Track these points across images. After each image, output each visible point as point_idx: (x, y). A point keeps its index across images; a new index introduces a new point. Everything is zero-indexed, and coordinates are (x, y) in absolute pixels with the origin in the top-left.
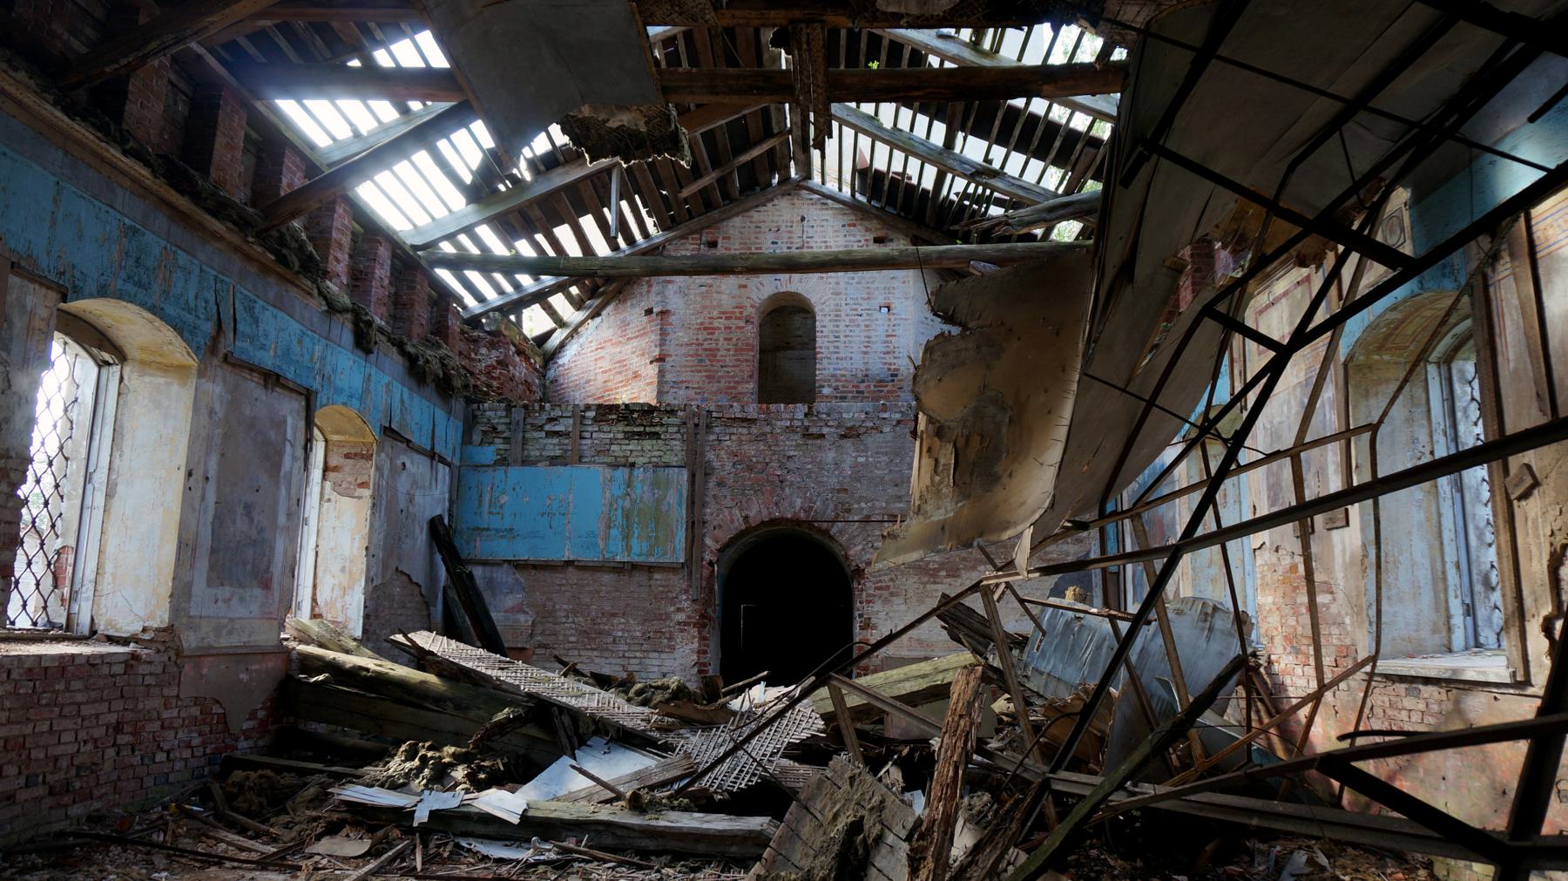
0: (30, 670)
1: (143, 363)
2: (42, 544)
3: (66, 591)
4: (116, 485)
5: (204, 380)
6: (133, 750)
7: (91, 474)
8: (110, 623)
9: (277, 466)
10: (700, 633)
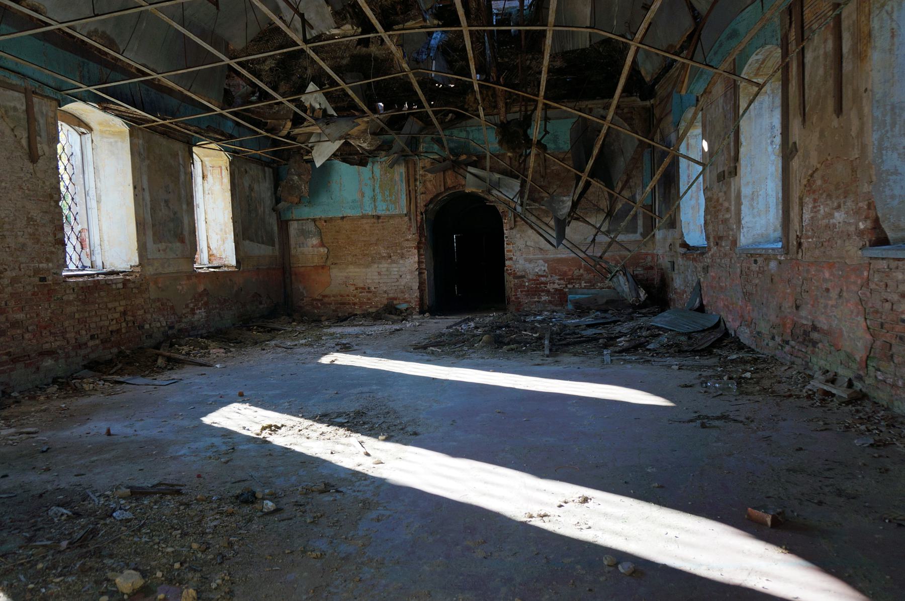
0: (82, 287)
1: (101, 132)
2: (72, 228)
3: (88, 250)
4: (101, 196)
5: (133, 138)
6: (134, 324)
7: (88, 191)
8: (111, 264)
9: (178, 178)
10: (419, 252)
